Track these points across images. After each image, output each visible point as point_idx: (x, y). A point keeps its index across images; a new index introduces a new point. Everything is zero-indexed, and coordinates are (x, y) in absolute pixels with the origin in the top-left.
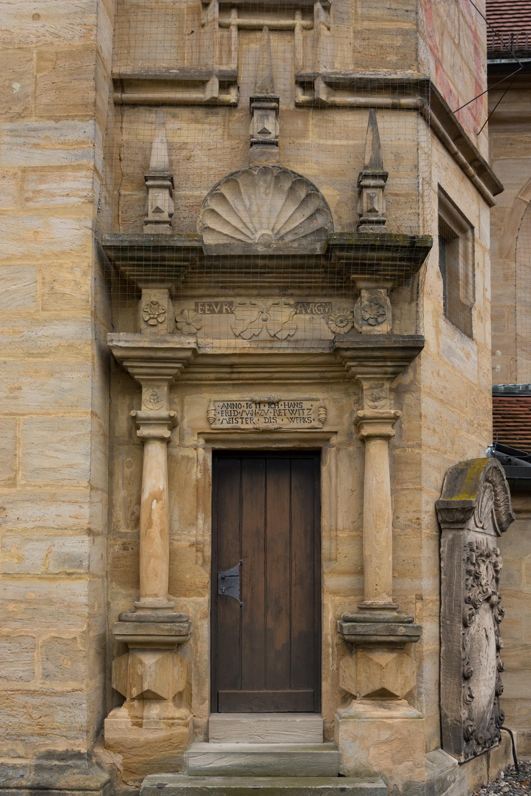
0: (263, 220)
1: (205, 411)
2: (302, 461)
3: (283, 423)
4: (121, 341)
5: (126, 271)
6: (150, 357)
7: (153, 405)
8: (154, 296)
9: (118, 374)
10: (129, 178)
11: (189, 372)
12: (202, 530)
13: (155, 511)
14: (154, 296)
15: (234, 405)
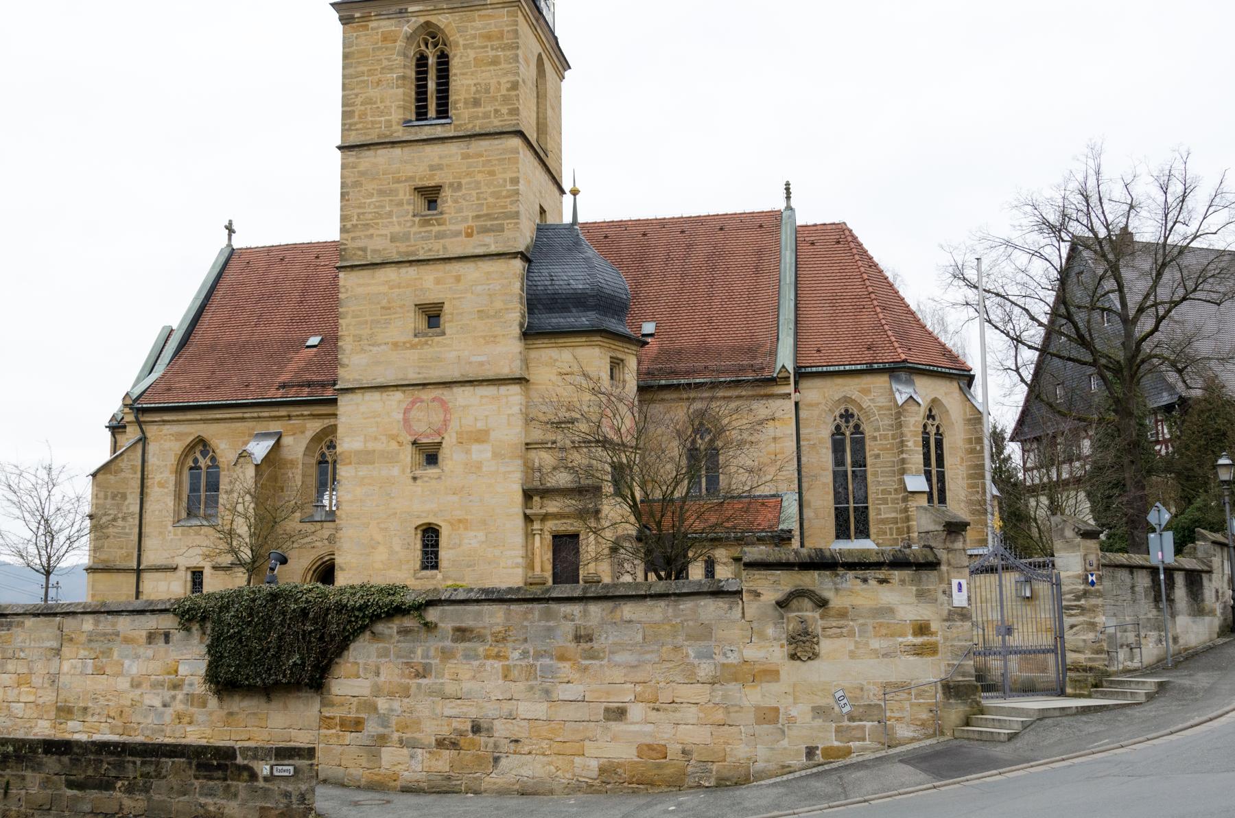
0: (563, 479)
1: (551, 525)
2: (575, 536)
4: (528, 512)
5: (528, 495)
6: (535, 515)
7: (537, 526)
8: (536, 499)
9: (528, 519)
10: (529, 468)
11: (544, 518)
12: (550, 555)
13: (537, 551)
14: (536, 499)
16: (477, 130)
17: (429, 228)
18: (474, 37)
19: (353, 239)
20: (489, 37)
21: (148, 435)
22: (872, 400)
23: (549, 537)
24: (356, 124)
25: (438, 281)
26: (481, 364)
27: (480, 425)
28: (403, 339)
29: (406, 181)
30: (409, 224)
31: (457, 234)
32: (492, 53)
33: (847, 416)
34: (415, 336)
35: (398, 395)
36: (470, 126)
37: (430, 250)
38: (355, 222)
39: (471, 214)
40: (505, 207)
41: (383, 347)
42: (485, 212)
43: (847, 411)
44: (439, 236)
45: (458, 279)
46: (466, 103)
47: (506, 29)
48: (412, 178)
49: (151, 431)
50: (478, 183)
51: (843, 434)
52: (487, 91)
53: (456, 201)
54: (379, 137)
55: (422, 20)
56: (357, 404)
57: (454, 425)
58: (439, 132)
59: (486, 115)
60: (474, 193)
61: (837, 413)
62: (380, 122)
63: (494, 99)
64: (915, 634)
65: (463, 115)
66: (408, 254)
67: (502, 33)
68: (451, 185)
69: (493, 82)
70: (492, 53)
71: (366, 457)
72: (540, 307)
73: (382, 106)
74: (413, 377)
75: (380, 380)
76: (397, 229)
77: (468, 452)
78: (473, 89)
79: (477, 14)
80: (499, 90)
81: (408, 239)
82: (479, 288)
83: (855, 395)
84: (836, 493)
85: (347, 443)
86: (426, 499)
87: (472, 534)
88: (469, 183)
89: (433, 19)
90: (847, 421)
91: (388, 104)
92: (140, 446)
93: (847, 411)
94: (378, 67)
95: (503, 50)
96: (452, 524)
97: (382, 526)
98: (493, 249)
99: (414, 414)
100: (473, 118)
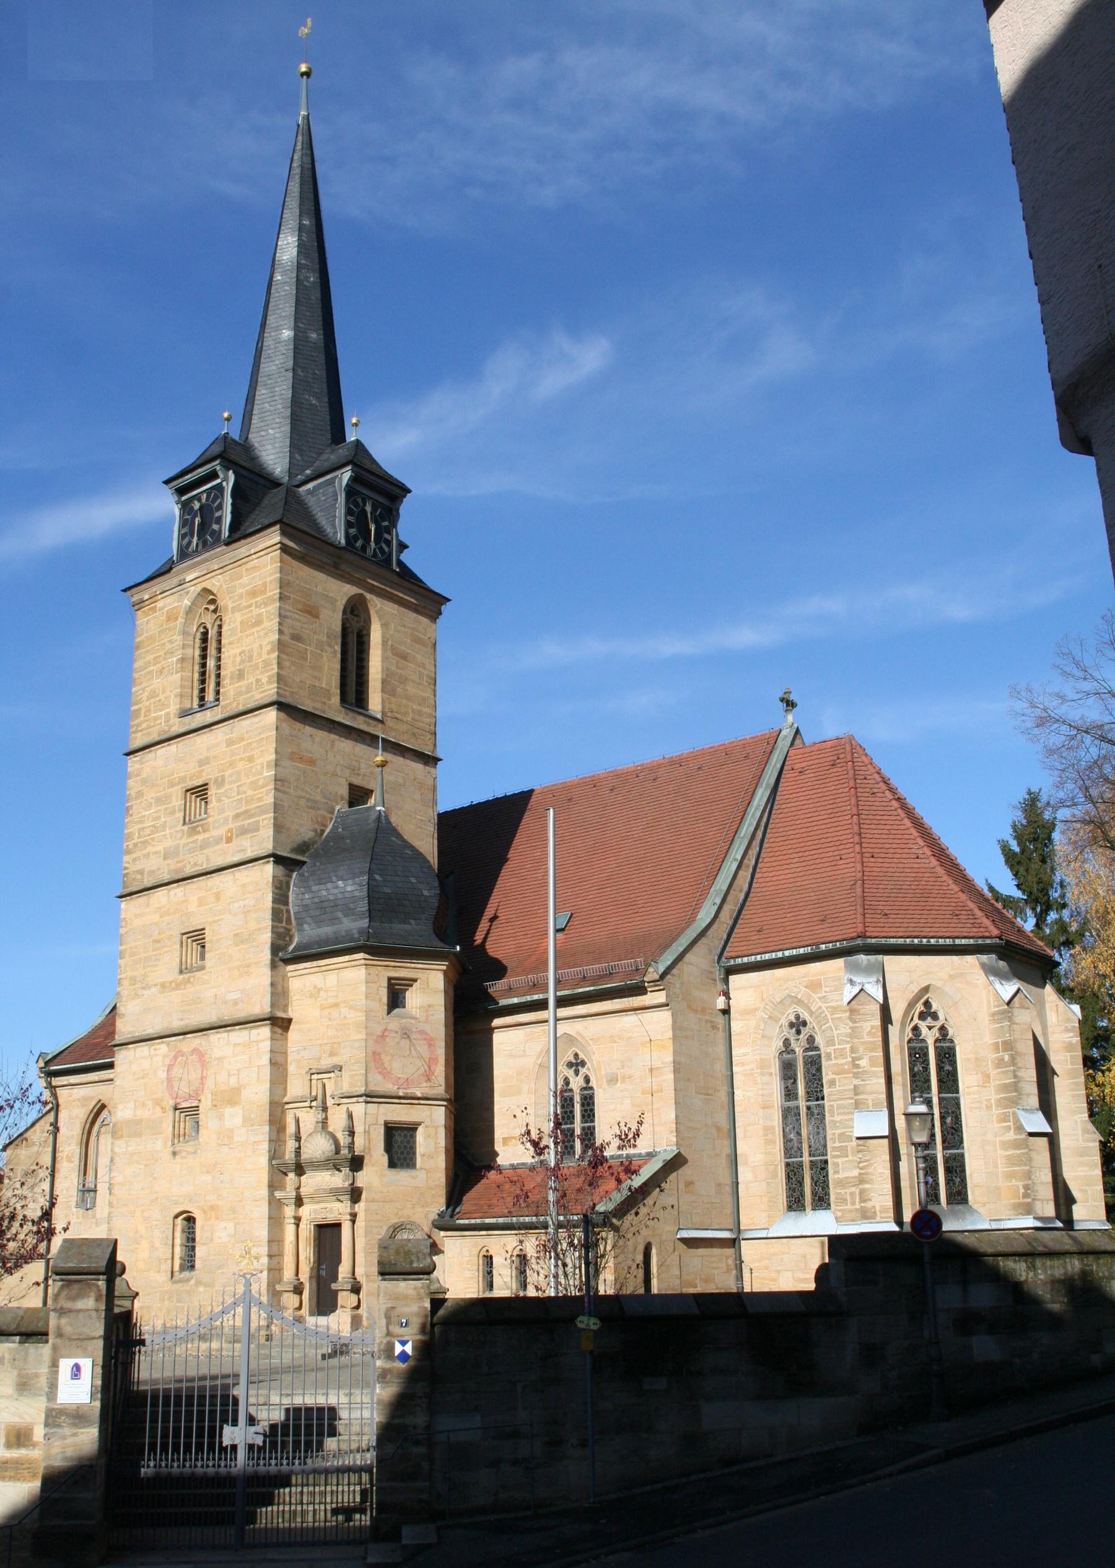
3: (329, 1215)
15: (315, 1210)
16: (241, 708)
17: (196, 837)
18: (241, 597)
19: (134, 860)
20: (253, 594)
21: (61, 1101)
22: (823, 999)
23: (307, 1231)
24: (142, 723)
25: (201, 902)
26: (235, 1003)
27: (233, 1082)
28: (170, 979)
29: (179, 783)
30: (180, 835)
31: (218, 841)
32: (258, 611)
33: (798, 1025)
34: (181, 972)
35: (162, 1048)
36: (234, 705)
37: (195, 864)
38: (136, 840)
39: (230, 813)
40: (260, 799)
41: (153, 990)
42: (244, 809)
43: (797, 1017)
44: (205, 845)
45: (218, 897)
46: (232, 678)
47: (269, 579)
48: (182, 779)
49: (62, 1093)
50: (239, 773)
51: (793, 1051)
52: (250, 658)
53: (219, 800)
54: (159, 735)
55: (199, 588)
56: (130, 1063)
57: (210, 1083)
58: (208, 716)
59: (249, 689)
60: (234, 786)
61: (784, 1022)
62: (160, 717)
63: (256, 667)
64: (9, 1445)
65: (234, 695)
66: (176, 871)
67: (265, 585)
68: (216, 780)
69: (256, 646)
70: (258, 611)
71: (136, 1128)
72: (308, 920)
73: (162, 697)
74: (177, 1025)
75: (150, 1031)
76: (169, 843)
77: (221, 1117)
78: (238, 659)
79: (244, 567)
80: (260, 655)
81: (177, 853)
82: (236, 904)
83: (802, 993)
84: (787, 1141)
85: (121, 1112)
86: (183, 1183)
87: (223, 1224)
88: (231, 776)
89: (207, 585)
90: (798, 1032)
91: (168, 694)
92: (53, 1113)
93: (797, 1017)
94: (161, 653)
95: (266, 604)
96: (205, 1212)
97: (146, 1214)
98: (250, 854)
99: (177, 1071)
100: (240, 694)
